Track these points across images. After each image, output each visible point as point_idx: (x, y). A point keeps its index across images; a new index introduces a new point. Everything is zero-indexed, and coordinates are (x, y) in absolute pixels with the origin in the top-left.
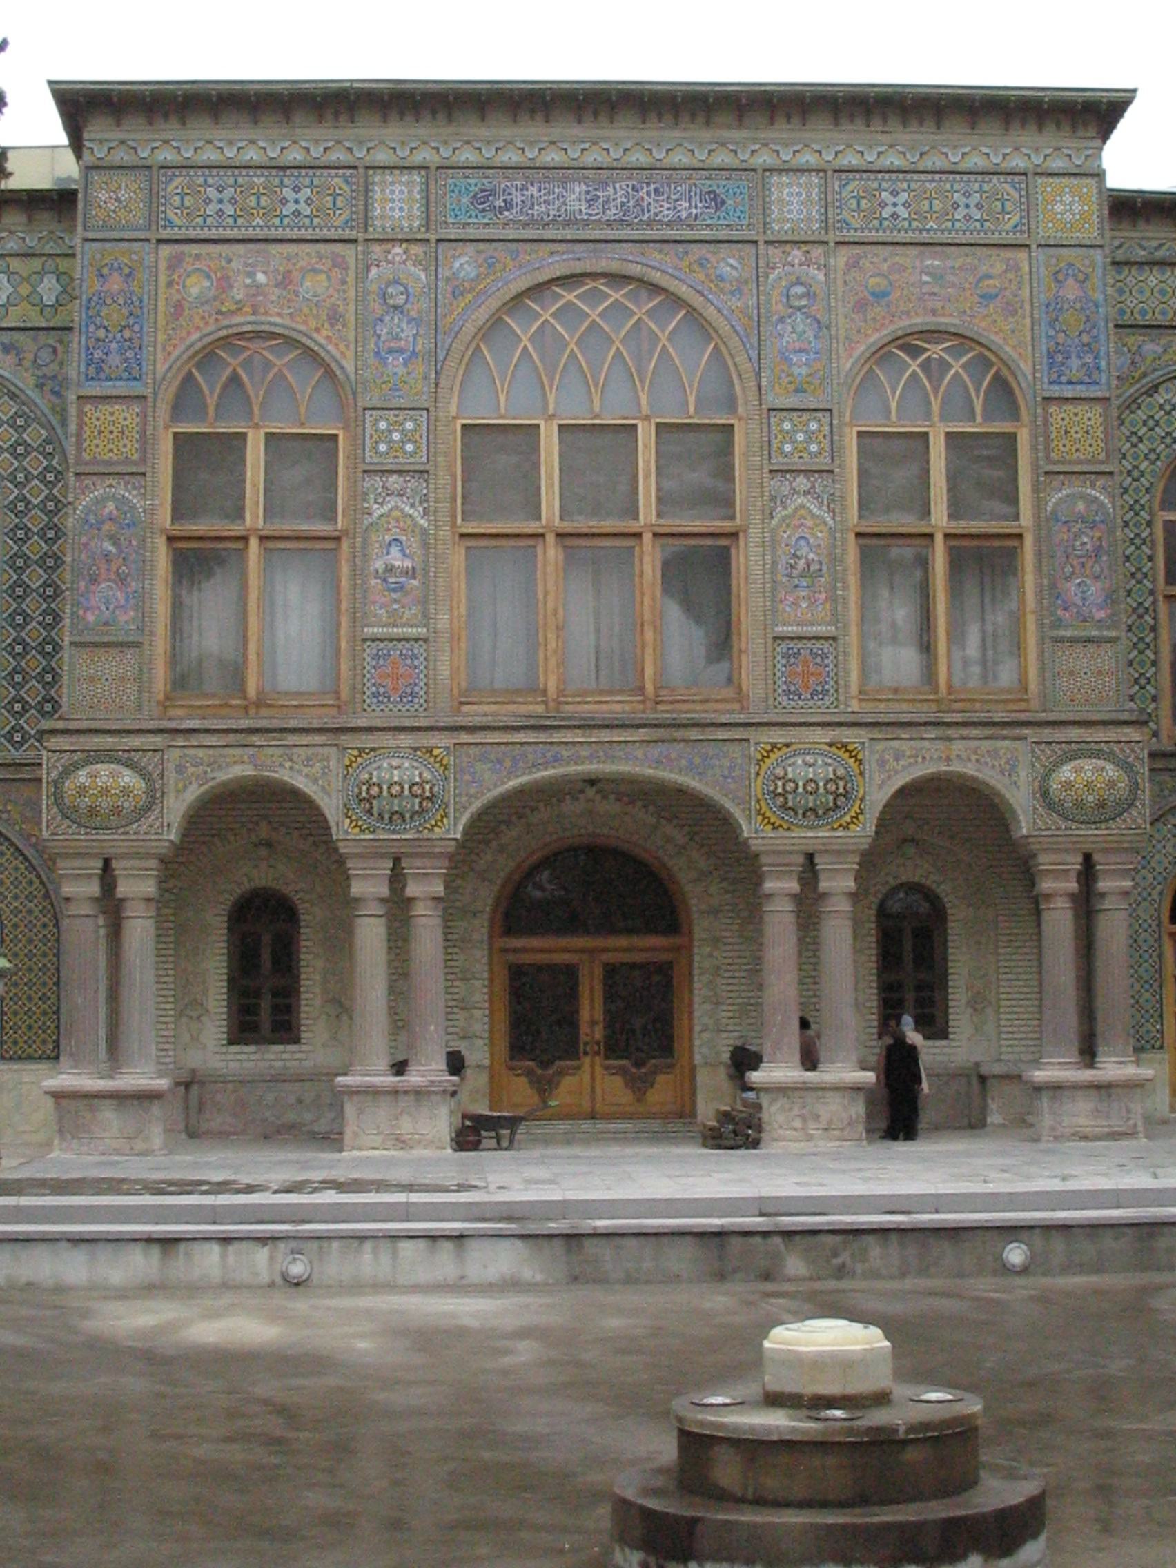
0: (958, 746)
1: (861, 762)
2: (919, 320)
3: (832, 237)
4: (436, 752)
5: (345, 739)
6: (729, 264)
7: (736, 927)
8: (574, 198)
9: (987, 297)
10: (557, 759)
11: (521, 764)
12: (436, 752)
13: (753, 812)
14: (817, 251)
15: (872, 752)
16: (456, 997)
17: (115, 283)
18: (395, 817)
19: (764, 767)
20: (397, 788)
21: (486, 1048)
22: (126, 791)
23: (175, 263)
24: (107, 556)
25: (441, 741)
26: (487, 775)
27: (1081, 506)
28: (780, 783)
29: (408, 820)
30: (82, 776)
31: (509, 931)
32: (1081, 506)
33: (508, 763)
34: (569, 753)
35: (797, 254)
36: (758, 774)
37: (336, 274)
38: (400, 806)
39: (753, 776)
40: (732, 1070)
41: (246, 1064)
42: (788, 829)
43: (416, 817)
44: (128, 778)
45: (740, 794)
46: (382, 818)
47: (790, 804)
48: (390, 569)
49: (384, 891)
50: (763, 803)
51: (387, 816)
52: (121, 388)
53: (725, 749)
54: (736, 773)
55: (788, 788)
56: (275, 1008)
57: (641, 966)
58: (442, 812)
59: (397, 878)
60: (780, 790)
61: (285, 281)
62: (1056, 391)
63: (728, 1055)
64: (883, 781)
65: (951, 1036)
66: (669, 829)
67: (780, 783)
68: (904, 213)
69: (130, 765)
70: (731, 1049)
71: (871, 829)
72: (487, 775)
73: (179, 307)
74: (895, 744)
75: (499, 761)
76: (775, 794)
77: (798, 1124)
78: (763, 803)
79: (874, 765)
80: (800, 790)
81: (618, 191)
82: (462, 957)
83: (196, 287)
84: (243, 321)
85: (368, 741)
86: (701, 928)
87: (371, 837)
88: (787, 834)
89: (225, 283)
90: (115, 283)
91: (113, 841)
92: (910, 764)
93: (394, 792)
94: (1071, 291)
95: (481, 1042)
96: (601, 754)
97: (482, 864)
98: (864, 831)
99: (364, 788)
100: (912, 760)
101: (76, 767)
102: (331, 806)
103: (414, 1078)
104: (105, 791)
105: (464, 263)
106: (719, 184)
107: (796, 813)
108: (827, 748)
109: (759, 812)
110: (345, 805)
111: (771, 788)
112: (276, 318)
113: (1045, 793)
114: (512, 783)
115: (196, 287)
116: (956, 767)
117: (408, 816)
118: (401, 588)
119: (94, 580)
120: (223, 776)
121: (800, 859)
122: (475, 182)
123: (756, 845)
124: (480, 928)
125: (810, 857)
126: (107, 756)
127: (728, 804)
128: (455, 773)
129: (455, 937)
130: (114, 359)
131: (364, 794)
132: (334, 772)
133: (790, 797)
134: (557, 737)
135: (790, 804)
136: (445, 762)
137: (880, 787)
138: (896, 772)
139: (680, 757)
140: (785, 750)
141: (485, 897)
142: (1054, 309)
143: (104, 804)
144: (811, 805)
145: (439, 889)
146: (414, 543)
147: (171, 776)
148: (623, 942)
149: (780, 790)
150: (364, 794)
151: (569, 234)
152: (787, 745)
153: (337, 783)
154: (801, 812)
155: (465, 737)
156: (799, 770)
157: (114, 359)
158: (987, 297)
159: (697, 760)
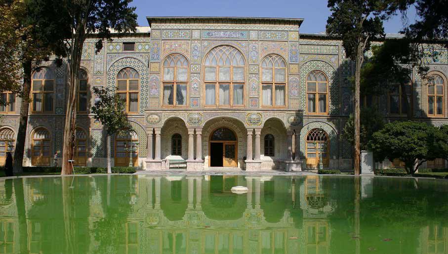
0: (276, 114)
2: (271, 52)
3: (259, 40)
5: (187, 111)
6: (244, 44)
10: (218, 115)
14: (257, 42)
17: (156, 46)
22: (156, 119)
23: (164, 43)
24: (154, 85)
27: (294, 79)
30: (150, 117)
31: (212, 140)
32: (294, 79)
35: (254, 42)
37: (187, 45)
44: (156, 117)
48: (194, 87)
49: (193, 133)
52: (156, 61)
56: (178, 150)
57: (230, 145)
61: (180, 46)
62: (291, 63)
66: (234, 125)
68: (269, 36)
69: (157, 115)
71: (263, 125)
73: (165, 49)
81: (228, 33)
83: (167, 46)
85: (191, 112)
86: (239, 139)
89: (171, 46)
90: (156, 46)
91: (155, 126)
94: (294, 48)
101: (149, 115)
102: (186, 121)
103: (197, 160)
104: (153, 119)
105: (206, 43)
106: (243, 32)
113: (288, 121)
114: (211, 118)
115: (167, 46)
116: (275, 117)
118: (196, 90)
119: (152, 89)
120: (170, 117)
122: (208, 32)
123: (246, 127)
124: (207, 139)
125: (254, 129)
126: (153, 114)
127: (242, 122)
130: (155, 57)
134: (218, 111)
141: (208, 135)
142: (291, 51)
143: (154, 121)
145: (201, 133)
146: (198, 83)
147: (163, 117)
148: (227, 141)
151: (221, 39)
155: (205, 111)
156: (254, 117)
157: (155, 57)
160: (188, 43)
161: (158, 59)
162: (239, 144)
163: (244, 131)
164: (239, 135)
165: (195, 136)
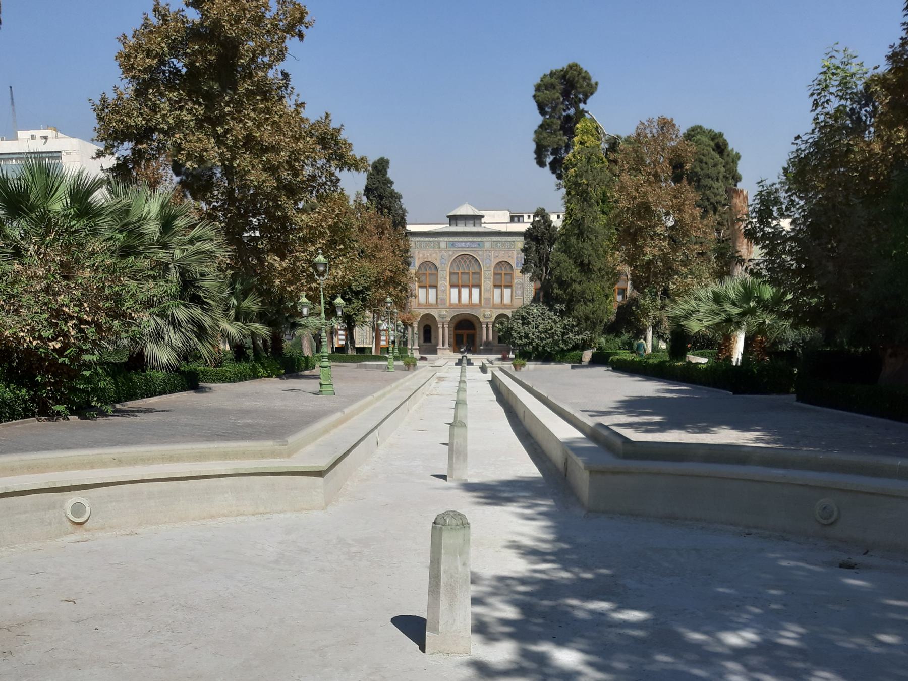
6: (480, 253)
8: (463, 244)
9: (509, 256)
25: (448, 309)
59: (443, 325)
61: (431, 255)
81: (468, 243)
84: (426, 260)
86: (478, 329)
89: (424, 255)
94: (519, 256)
98: (493, 320)
103: (445, 347)
105: (451, 253)
112: (430, 260)
115: (421, 255)
124: (452, 329)
141: (453, 325)
142: (517, 258)
158: (509, 256)
160: (437, 253)
161: (414, 266)
162: (478, 333)
163: (481, 323)
164: (477, 326)
165: (443, 328)
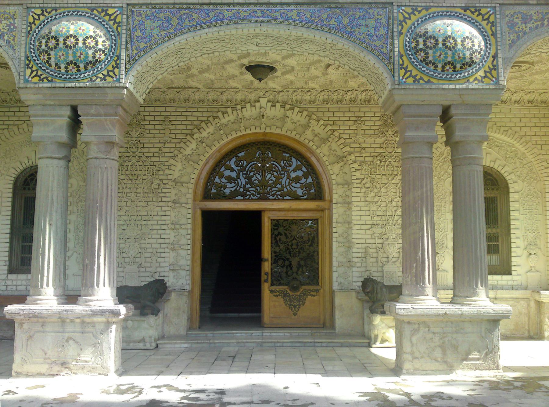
1: (493, 24)
4: (110, 11)
7: (362, 195)
11: (187, 22)
12: (110, 11)
13: (396, 66)
15: (503, 16)
16: (167, 241)
18: (70, 67)
19: (406, 27)
20: (73, 40)
21: (188, 278)
26: (156, 32)
28: (421, 40)
29: (82, 70)
33: (175, 22)
34: (230, 14)
36: (400, 33)
38: (74, 56)
39: (396, 34)
40: (362, 296)
41: (19, 288)
42: (429, 81)
43: (89, 68)
45: (384, 50)
46: (59, 68)
47: (430, 59)
50: (404, 58)
51: (63, 66)
53: (371, 11)
54: (382, 31)
55: (429, 44)
58: (114, 63)
60: (421, 46)
63: (360, 284)
64: (513, 41)
65: (513, 273)
67: (421, 40)
70: (362, 279)
72: (156, 32)
74: (523, 9)
75: (167, 19)
76: (416, 50)
77: (438, 354)
78: (404, 58)
79: (505, 28)
80: (440, 45)
82: (173, 214)
87: (49, 85)
88: (428, 86)
92: (537, 27)
93: (69, 43)
95: (183, 273)
96: (259, 14)
97: (188, 151)
99: (44, 41)
100: (539, 23)
107: (436, 67)
108: (462, 11)
109: (402, 66)
110: (27, 57)
111: (413, 45)
117: (82, 66)
121: (440, 112)
128: (127, 30)
129: (168, 199)
131: (43, 47)
132: (19, 29)
133: (430, 52)
135: (430, 59)
136: (118, 20)
137: (511, 46)
138: (525, 33)
139: (329, 18)
140: (424, 12)
144: (449, 59)
149: (421, 46)
150: (43, 47)
152: (427, 8)
153: (22, 38)
154: (440, 66)
159: (346, 21)
